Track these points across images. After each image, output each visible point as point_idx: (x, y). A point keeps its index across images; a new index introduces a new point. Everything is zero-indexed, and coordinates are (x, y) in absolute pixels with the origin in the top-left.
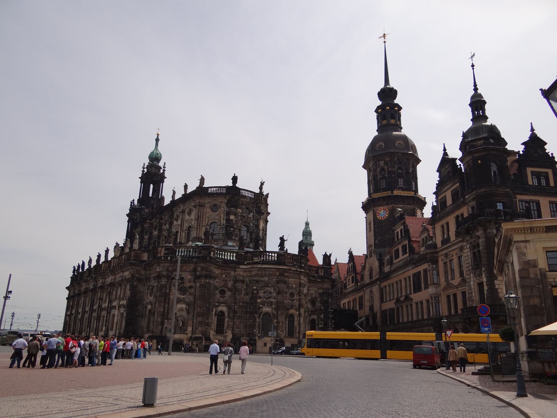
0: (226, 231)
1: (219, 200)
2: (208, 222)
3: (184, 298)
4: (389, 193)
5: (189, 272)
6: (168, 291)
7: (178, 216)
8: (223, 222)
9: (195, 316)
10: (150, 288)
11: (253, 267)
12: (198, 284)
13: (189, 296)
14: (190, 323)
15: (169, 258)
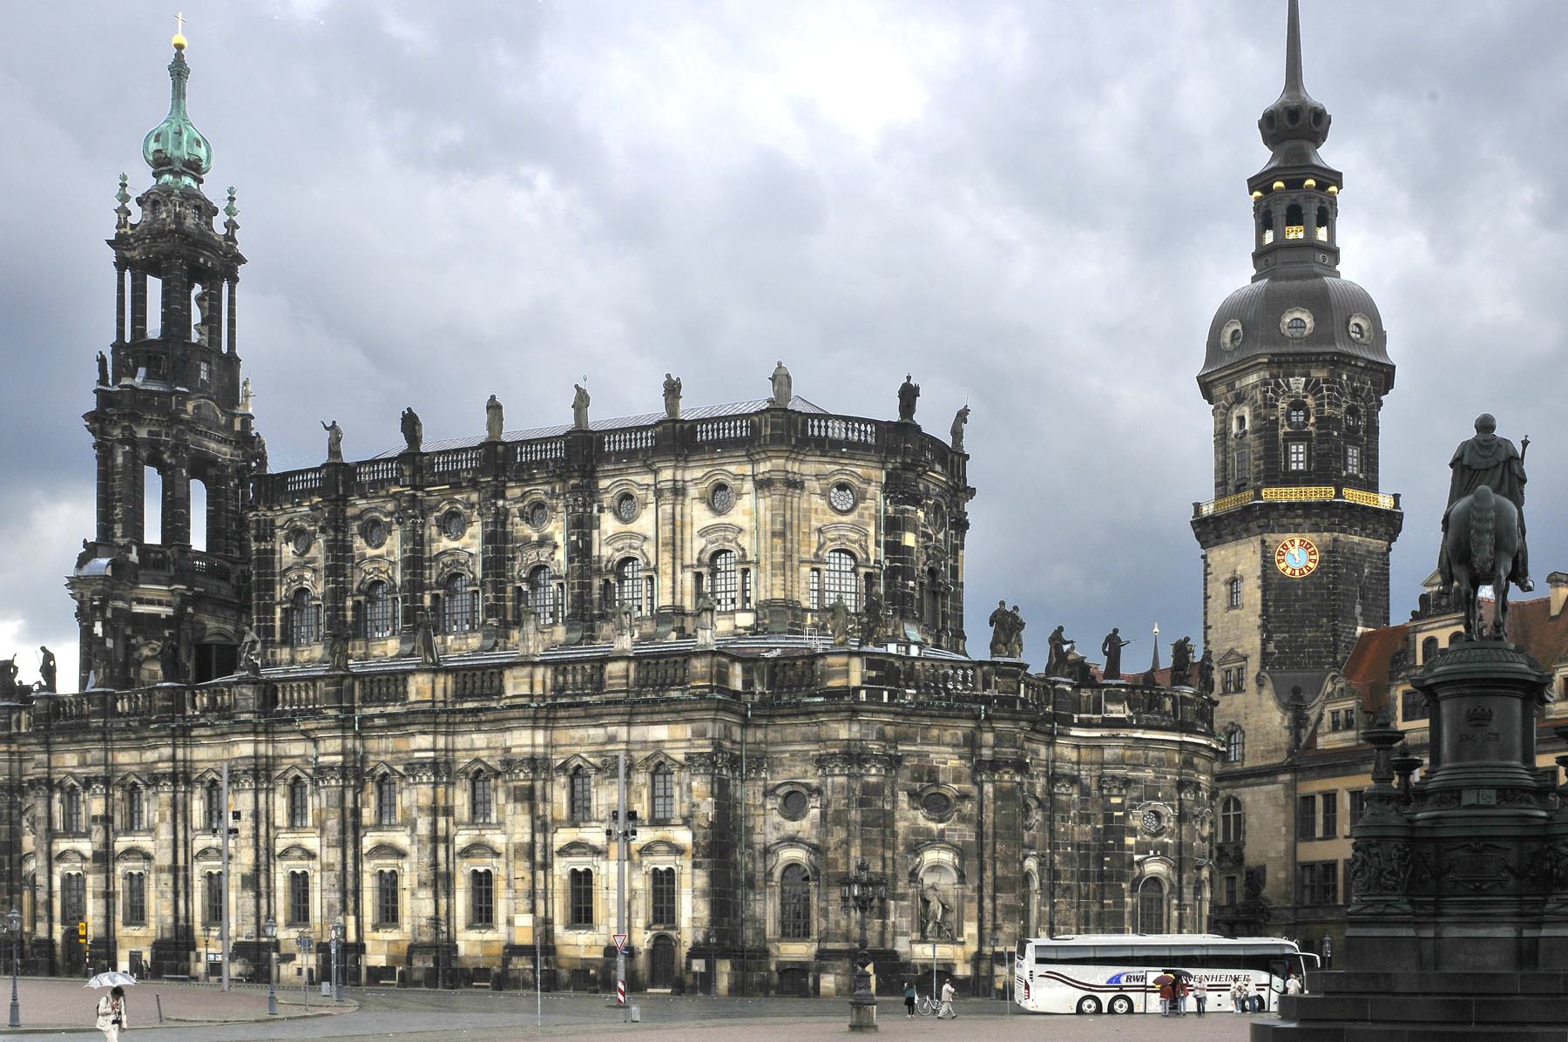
0: (887, 586)
1: (859, 471)
2: (821, 546)
3: (942, 832)
4: (1325, 493)
5: (955, 746)
6: (888, 807)
7: (627, 497)
8: (876, 553)
9: (988, 891)
10: (782, 791)
11: (1114, 737)
12: (988, 788)
13: (960, 826)
14: (971, 909)
15: (886, 694)
